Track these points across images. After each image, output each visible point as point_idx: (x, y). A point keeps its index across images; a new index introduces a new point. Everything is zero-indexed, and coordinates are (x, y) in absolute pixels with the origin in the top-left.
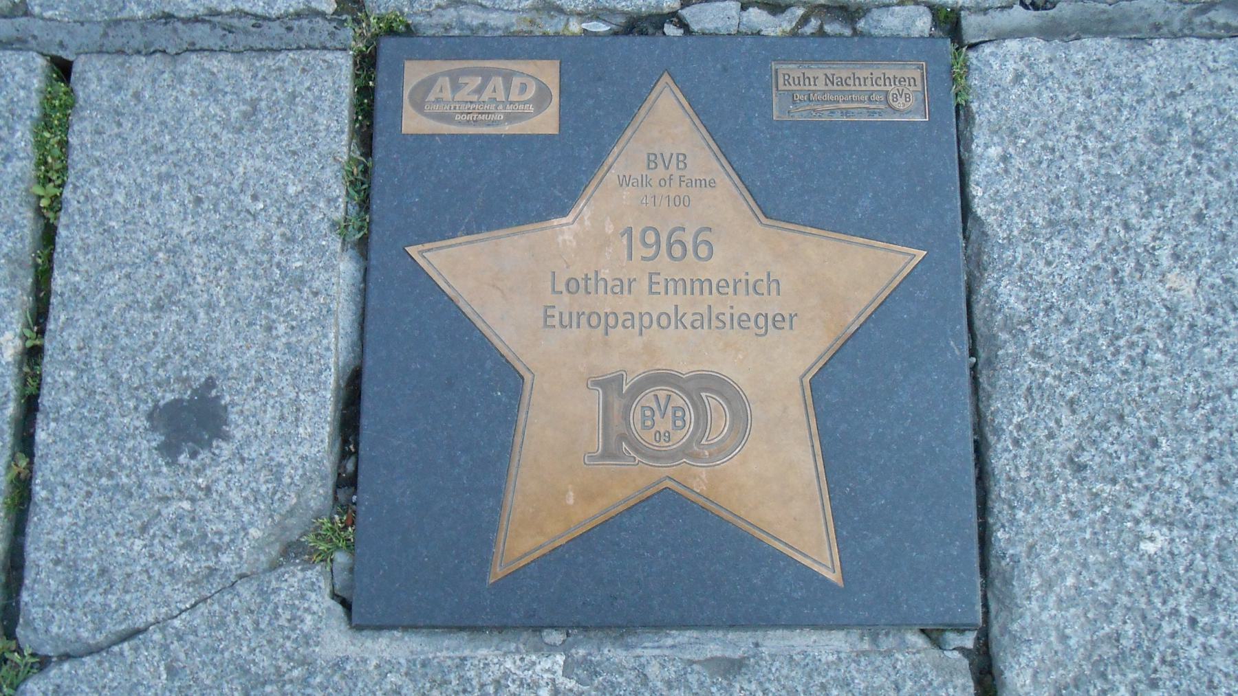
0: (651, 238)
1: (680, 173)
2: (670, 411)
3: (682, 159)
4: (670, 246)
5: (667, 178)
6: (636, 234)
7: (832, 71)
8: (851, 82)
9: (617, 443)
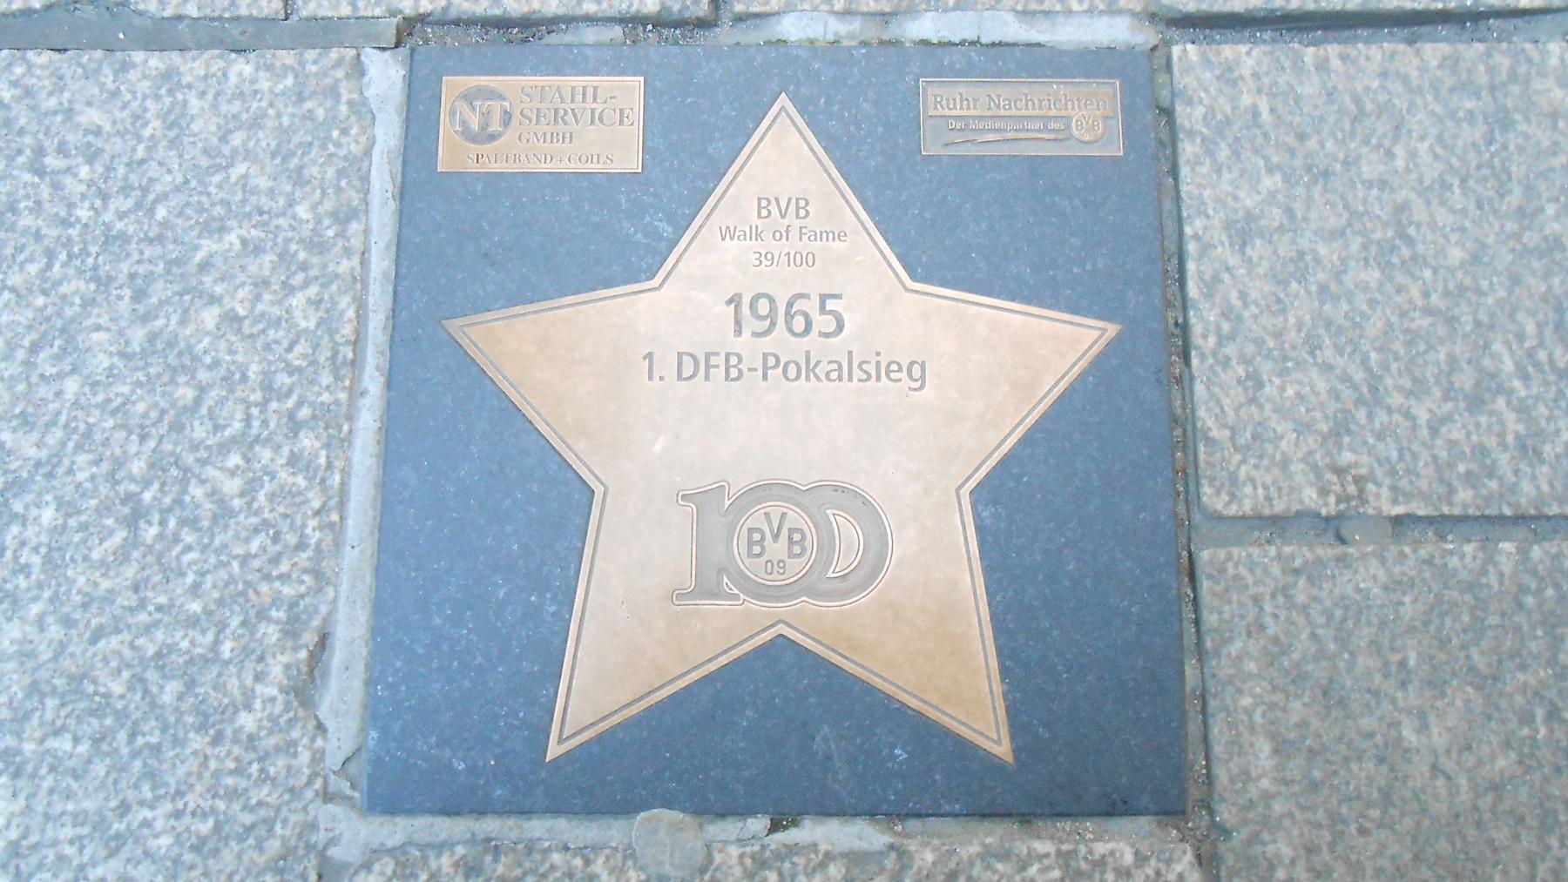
0: (763, 307)
2: (785, 532)
3: (801, 206)
4: (789, 316)
6: (746, 301)
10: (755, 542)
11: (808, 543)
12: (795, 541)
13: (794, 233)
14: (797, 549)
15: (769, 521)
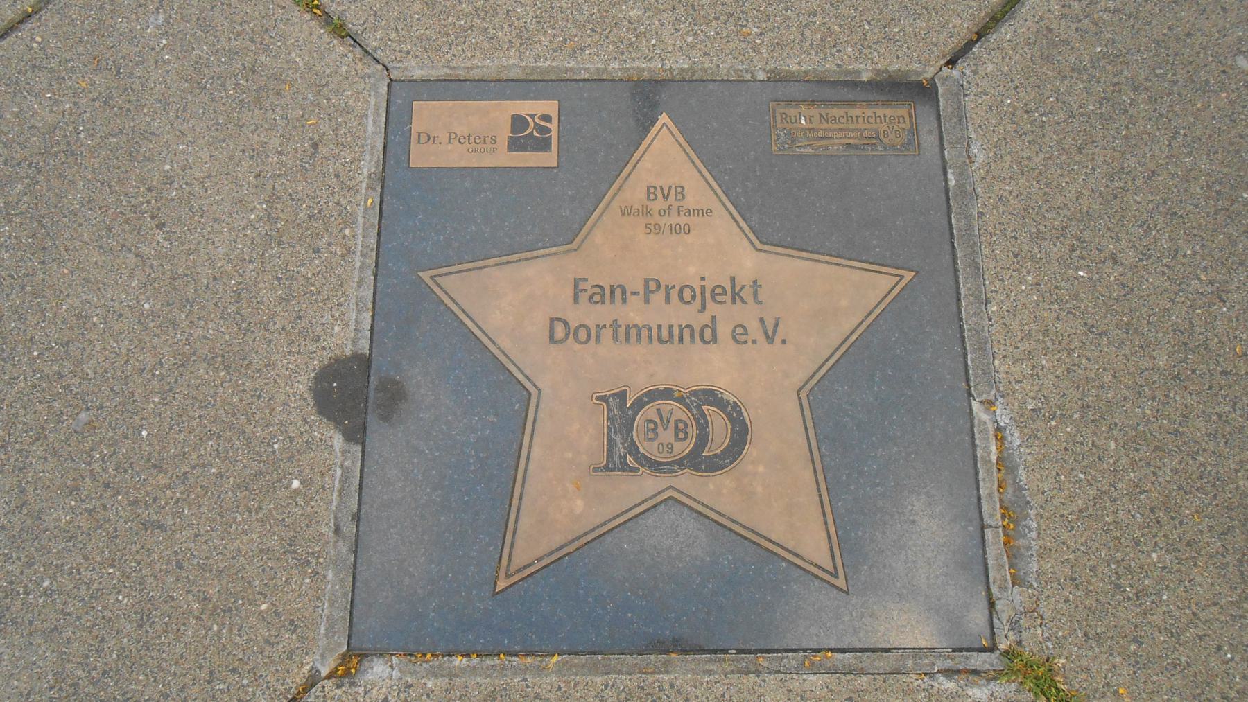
1: (680, 203)
2: (672, 424)
3: (680, 191)
5: (666, 208)
7: (829, 111)
9: (620, 456)
10: (652, 429)
11: (689, 430)
12: (680, 431)
14: (681, 435)
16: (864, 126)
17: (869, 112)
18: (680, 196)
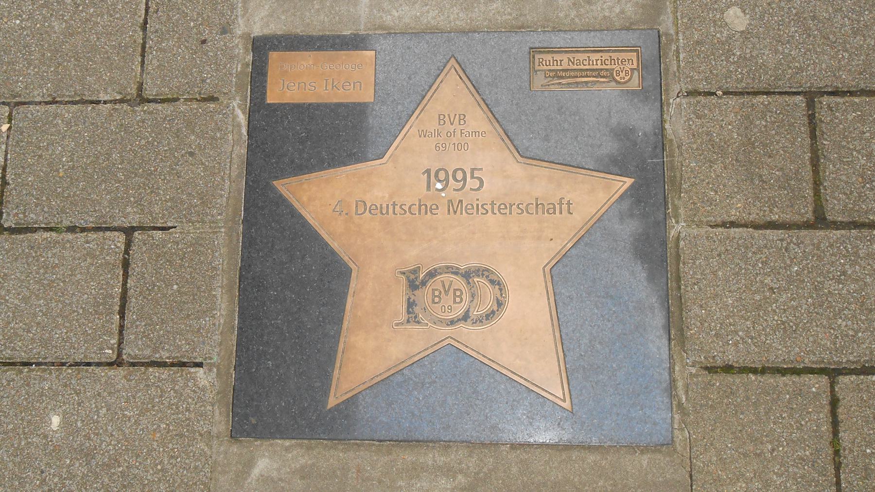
1: (462, 127)
8: (586, 63)
13: (458, 133)
15: (444, 286)
16: (602, 67)
17: (605, 56)
18: (462, 122)
